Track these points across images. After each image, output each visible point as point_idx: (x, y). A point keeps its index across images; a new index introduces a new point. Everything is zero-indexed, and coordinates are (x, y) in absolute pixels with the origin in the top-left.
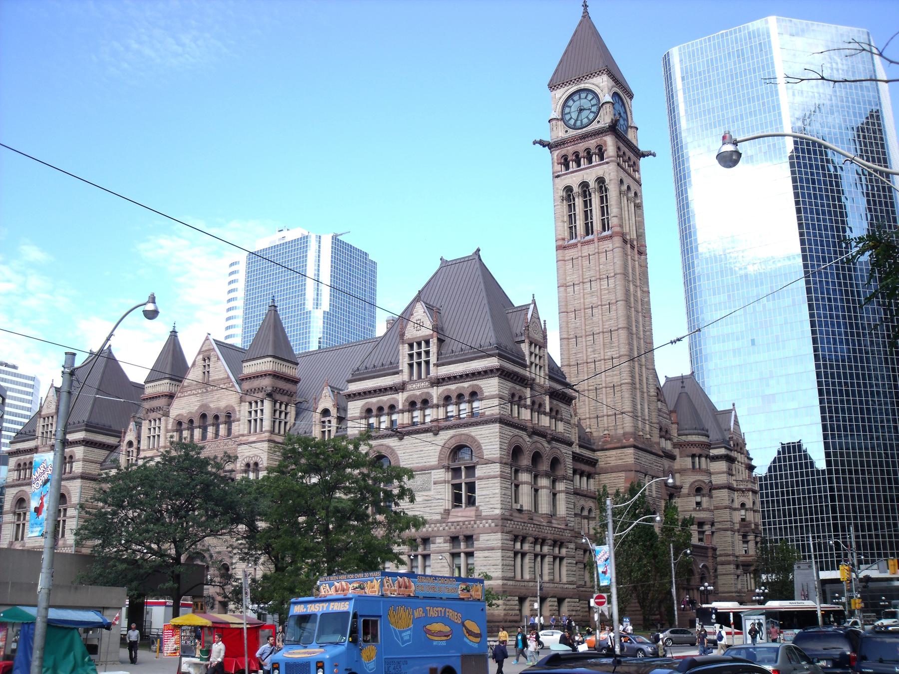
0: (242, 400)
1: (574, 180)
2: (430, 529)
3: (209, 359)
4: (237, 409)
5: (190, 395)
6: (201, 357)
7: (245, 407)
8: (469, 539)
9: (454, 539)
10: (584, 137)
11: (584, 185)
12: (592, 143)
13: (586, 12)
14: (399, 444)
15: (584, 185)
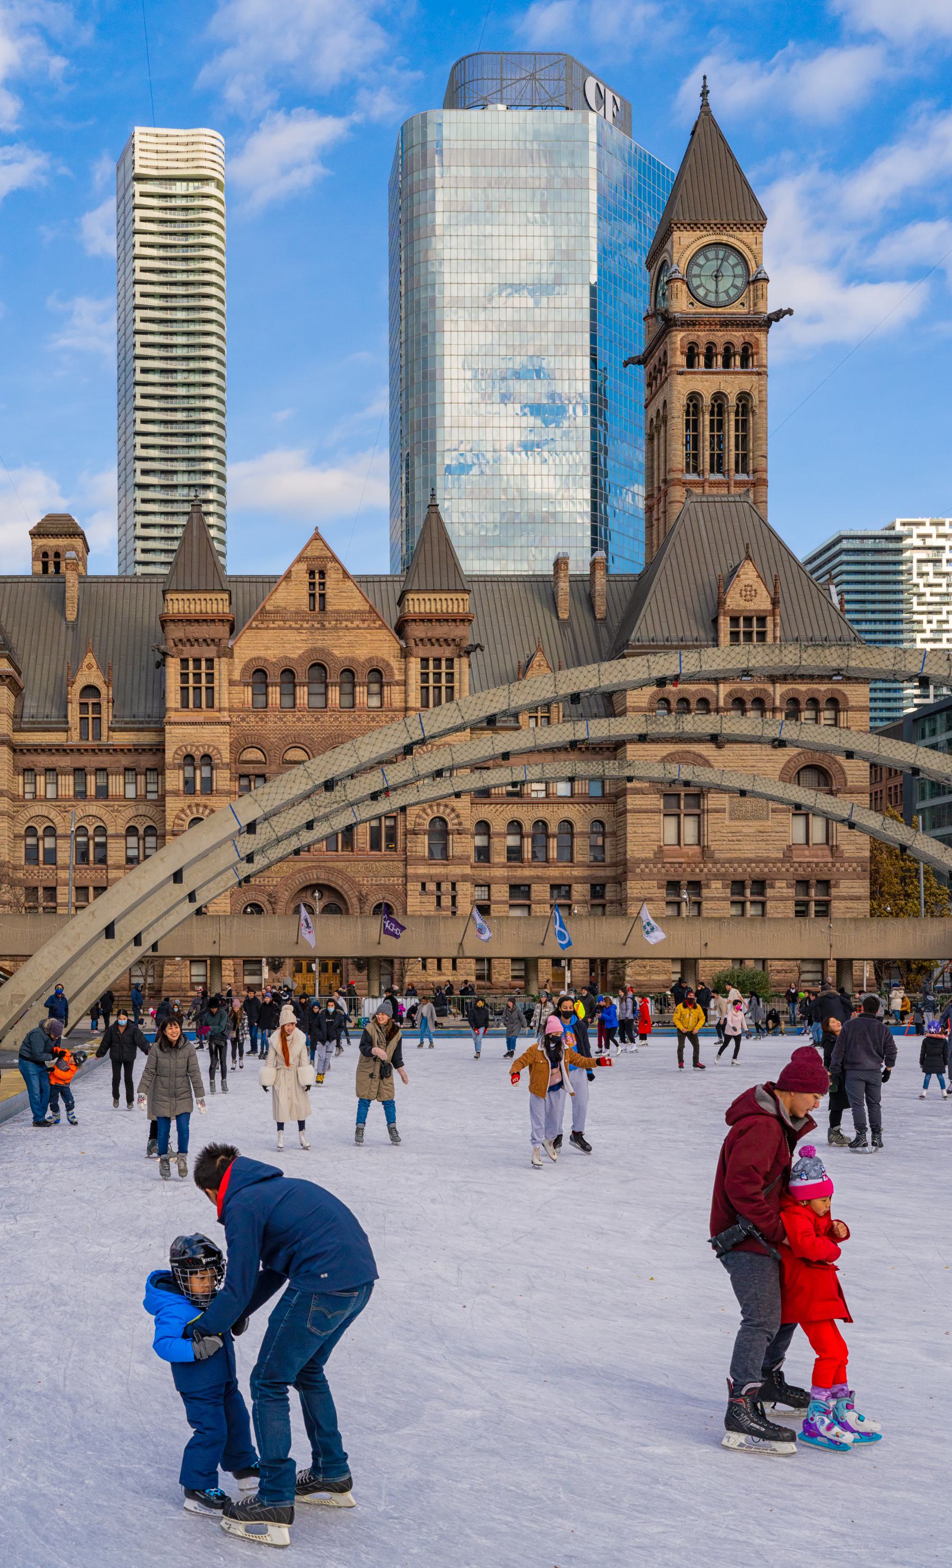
0: (405, 654)
1: (706, 385)
2: (766, 870)
3: (322, 574)
4: (395, 664)
5: (280, 628)
6: (303, 566)
7: (415, 665)
8: (825, 885)
9: (803, 884)
10: (727, 323)
11: (719, 397)
12: (737, 337)
13: (705, 105)
14: (716, 753)
15: (719, 397)
